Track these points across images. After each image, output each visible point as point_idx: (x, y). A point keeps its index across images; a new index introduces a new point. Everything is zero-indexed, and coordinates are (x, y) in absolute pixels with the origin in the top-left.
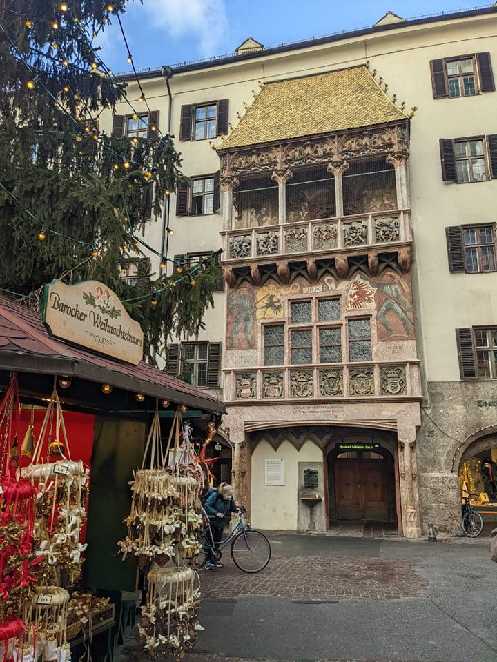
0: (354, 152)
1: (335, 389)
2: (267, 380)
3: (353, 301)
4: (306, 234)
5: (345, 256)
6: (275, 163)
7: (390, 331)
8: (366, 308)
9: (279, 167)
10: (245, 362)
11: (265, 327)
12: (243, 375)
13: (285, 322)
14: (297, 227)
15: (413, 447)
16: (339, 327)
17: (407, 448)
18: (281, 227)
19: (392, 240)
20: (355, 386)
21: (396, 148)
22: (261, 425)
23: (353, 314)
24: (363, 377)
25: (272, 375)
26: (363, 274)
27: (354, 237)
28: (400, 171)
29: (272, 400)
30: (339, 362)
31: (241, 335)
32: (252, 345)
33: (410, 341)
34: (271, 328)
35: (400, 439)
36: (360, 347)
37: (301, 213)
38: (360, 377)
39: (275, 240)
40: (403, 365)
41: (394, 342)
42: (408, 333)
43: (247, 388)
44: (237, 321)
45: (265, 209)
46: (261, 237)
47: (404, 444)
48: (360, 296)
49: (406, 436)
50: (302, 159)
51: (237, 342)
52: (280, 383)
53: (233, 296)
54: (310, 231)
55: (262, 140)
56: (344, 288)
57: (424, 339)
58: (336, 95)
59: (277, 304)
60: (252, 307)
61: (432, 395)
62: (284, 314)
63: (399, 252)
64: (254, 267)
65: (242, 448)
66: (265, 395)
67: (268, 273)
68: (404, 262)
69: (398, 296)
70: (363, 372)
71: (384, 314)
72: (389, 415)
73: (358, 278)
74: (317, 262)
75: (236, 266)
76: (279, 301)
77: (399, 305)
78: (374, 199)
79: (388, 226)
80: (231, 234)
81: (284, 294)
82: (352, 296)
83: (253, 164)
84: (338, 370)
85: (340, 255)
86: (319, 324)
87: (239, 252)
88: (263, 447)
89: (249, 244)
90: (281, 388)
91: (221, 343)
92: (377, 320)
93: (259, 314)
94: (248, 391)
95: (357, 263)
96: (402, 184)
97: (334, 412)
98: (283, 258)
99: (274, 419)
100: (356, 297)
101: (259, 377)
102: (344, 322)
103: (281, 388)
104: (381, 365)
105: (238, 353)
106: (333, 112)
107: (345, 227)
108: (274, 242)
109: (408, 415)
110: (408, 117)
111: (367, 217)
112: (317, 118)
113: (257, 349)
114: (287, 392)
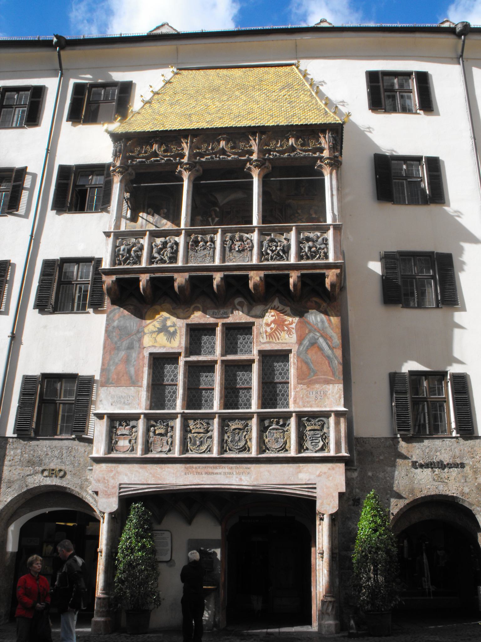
0: (277, 152)
1: (242, 444)
2: (152, 428)
5: (262, 273)
8: (284, 341)
10: (124, 403)
11: (154, 358)
13: (180, 354)
18: (183, 232)
19: (319, 258)
23: (268, 347)
24: (277, 429)
26: (284, 298)
27: (272, 251)
29: (157, 456)
30: (247, 408)
32: (134, 382)
33: (337, 385)
35: (319, 507)
37: (210, 219)
38: (273, 429)
39: (175, 247)
40: (327, 415)
41: (317, 386)
42: (334, 374)
43: (124, 439)
44: (118, 349)
45: (165, 210)
47: (323, 515)
48: (278, 325)
50: (215, 154)
51: (115, 377)
52: (169, 434)
53: (115, 314)
54: (218, 238)
57: (352, 384)
58: (259, 90)
59: (172, 330)
60: (138, 332)
61: (359, 453)
62: (180, 343)
63: (326, 274)
69: (324, 328)
70: (278, 423)
71: (307, 349)
72: (308, 478)
74: (225, 279)
76: (174, 325)
77: (325, 339)
78: (299, 211)
83: (155, 154)
85: (255, 272)
86: (224, 358)
87: (127, 259)
89: (141, 249)
90: (170, 440)
92: (298, 356)
93: (147, 341)
96: (332, 195)
97: (238, 473)
99: (160, 482)
100: (273, 325)
103: (170, 440)
104: (300, 415)
106: (255, 107)
108: (172, 247)
109: (331, 478)
110: (340, 122)
111: (289, 230)
112: (236, 111)
113: (141, 386)
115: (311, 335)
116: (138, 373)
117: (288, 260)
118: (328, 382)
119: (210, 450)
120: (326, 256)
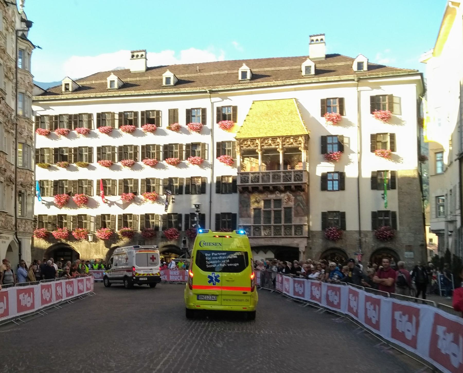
1: (279, 233)
3: (286, 201)
4: (269, 176)
5: (284, 186)
16: (280, 211)
17: (302, 254)
20: (286, 232)
23: (286, 206)
25: (257, 228)
31: (245, 212)
35: (300, 250)
36: (288, 219)
40: (302, 225)
44: (243, 207)
46: (252, 175)
56: (283, 196)
59: (258, 201)
61: (312, 235)
66: (254, 235)
67: (255, 190)
75: (243, 186)
76: (259, 200)
79: (298, 175)
81: (261, 197)
82: (286, 199)
87: (244, 181)
89: (248, 178)
91: (236, 214)
95: (288, 188)
98: (261, 185)
100: (287, 200)
102: (283, 209)
104: (295, 225)
115: (298, 203)
117: (291, 182)
119: (271, 235)
120: (302, 180)
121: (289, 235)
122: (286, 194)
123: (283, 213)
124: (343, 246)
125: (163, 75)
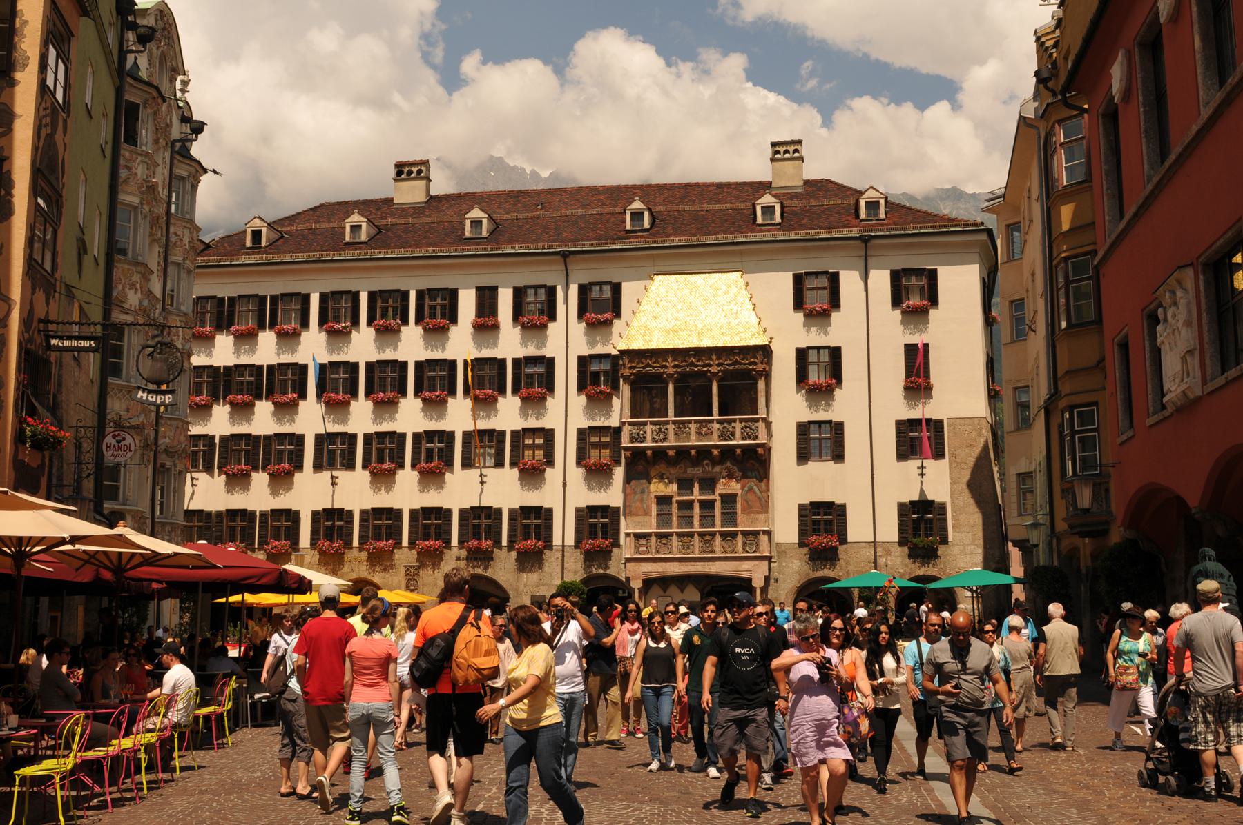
6: (666, 367)
7: (750, 507)
9: (671, 371)
12: (638, 536)
14: (683, 422)
15: (762, 589)
16: (714, 501)
17: (758, 592)
21: (760, 367)
22: (655, 575)
23: (724, 492)
28: (761, 385)
31: (638, 504)
32: (647, 513)
34: (663, 501)
36: (730, 518)
44: (635, 493)
46: (654, 428)
49: (758, 583)
55: (653, 345)
64: (649, 452)
65: (640, 592)
68: (761, 455)
73: (728, 464)
74: (698, 452)
80: (630, 424)
83: (648, 365)
84: (713, 534)
88: (656, 589)
94: (644, 549)
101: (653, 539)
102: (718, 498)
105: (637, 519)
107: (721, 427)
111: (734, 421)
114: (675, 550)
116: (649, 507)
117: (735, 439)
118: (759, 513)
120: (756, 438)
121: (732, 552)
122: (724, 466)
123: (718, 505)
124: (841, 574)
125: (467, 216)
